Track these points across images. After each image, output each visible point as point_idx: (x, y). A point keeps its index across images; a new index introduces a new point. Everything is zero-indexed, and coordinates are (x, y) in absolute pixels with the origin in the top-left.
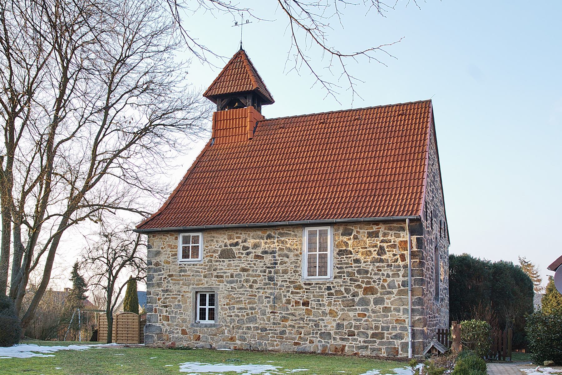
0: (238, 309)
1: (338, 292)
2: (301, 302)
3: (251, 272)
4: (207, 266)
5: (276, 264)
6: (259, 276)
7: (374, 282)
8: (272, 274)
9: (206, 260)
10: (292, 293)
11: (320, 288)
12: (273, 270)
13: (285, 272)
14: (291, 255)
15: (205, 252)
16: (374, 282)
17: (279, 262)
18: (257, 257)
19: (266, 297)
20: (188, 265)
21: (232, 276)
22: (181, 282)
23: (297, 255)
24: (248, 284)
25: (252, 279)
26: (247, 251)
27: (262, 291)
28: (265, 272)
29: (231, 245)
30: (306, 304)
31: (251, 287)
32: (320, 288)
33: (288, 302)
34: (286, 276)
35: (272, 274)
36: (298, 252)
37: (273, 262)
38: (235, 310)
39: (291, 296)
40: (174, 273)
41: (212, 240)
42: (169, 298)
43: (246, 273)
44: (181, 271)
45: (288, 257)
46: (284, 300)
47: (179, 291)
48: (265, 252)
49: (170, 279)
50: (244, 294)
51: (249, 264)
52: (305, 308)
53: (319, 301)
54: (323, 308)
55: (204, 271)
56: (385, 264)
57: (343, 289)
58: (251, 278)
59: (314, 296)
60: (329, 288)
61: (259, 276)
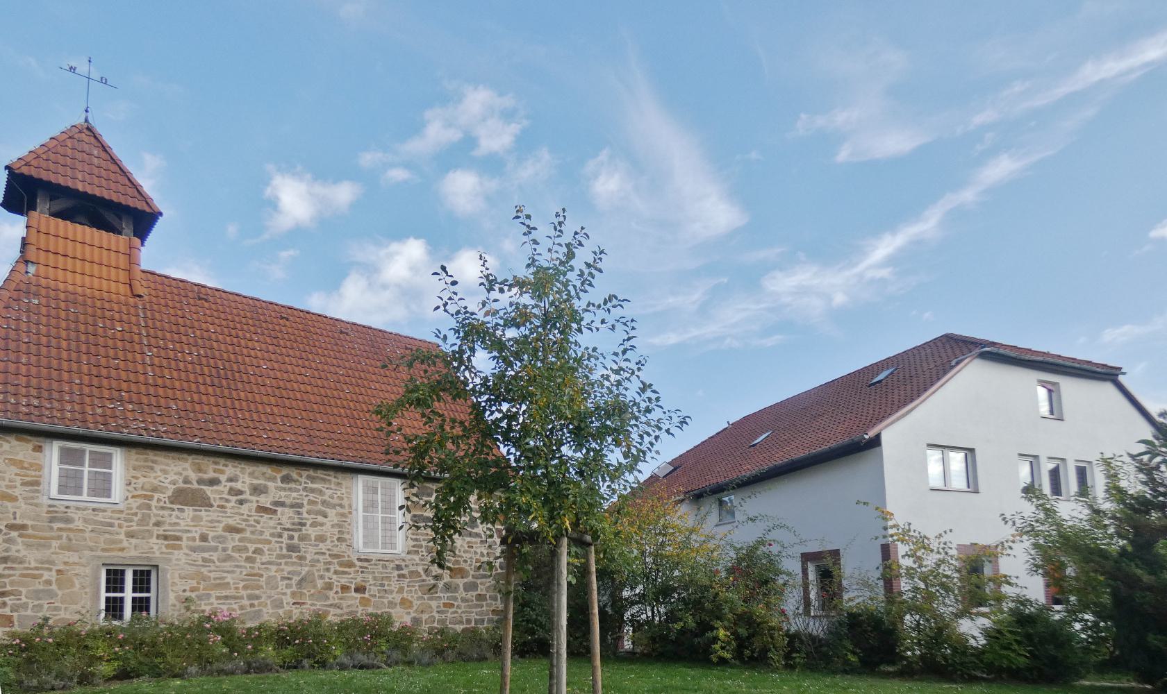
0: (218, 598)
1: (414, 574)
2: (353, 586)
3: (248, 535)
4: (136, 514)
5: (304, 525)
6: (270, 542)
7: (465, 561)
8: (296, 541)
9: (134, 504)
10: (336, 572)
11: (385, 567)
12: (296, 535)
13: (321, 539)
14: (331, 513)
15: (130, 488)
16: (465, 561)
17: (309, 523)
18: (262, 509)
19: (283, 578)
20: (78, 509)
21: (204, 538)
22: (55, 543)
23: (343, 515)
24: (244, 556)
25: (252, 547)
26: (240, 497)
27: (274, 568)
28: (280, 536)
29: (200, 482)
30: (360, 589)
31: (248, 559)
32: (385, 567)
33: (329, 587)
34: (321, 545)
35: (296, 541)
36: (346, 511)
37: (296, 521)
38: (213, 600)
39: (334, 577)
40: (29, 523)
41: (152, 468)
42: (10, 576)
43: (237, 536)
44: (52, 520)
45: (326, 517)
46: (320, 583)
47: (48, 562)
48: (282, 504)
49: (14, 534)
50: (233, 572)
51: (244, 520)
52: (358, 595)
53: (382, 585)
54: (390, 597)
55: (126, 524)
56: (478, 540)
57: (420, 569)
58: (249, 545)
59: (375, 578)
60: (399, 568)
61: (270, 542)
